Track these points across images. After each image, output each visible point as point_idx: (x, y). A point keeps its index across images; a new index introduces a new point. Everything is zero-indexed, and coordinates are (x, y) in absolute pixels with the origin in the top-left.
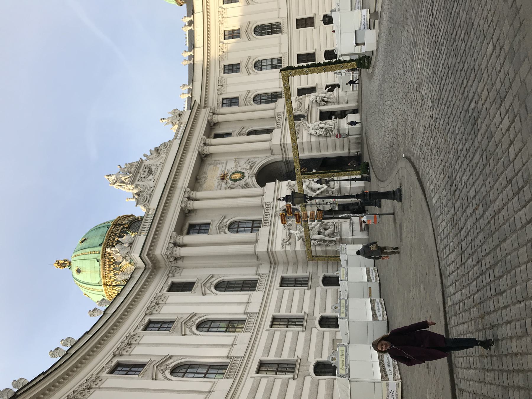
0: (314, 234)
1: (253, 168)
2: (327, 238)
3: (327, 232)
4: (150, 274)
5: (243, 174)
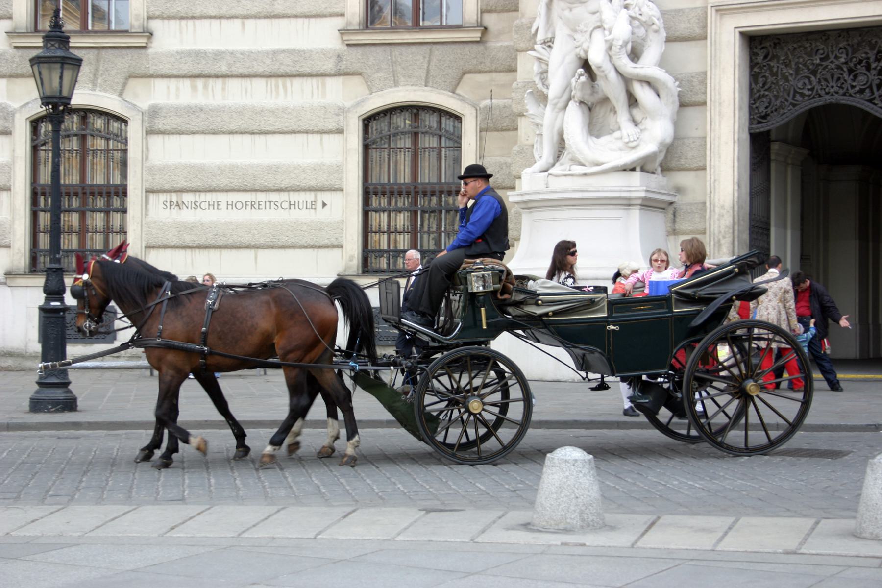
3: (574, 121)
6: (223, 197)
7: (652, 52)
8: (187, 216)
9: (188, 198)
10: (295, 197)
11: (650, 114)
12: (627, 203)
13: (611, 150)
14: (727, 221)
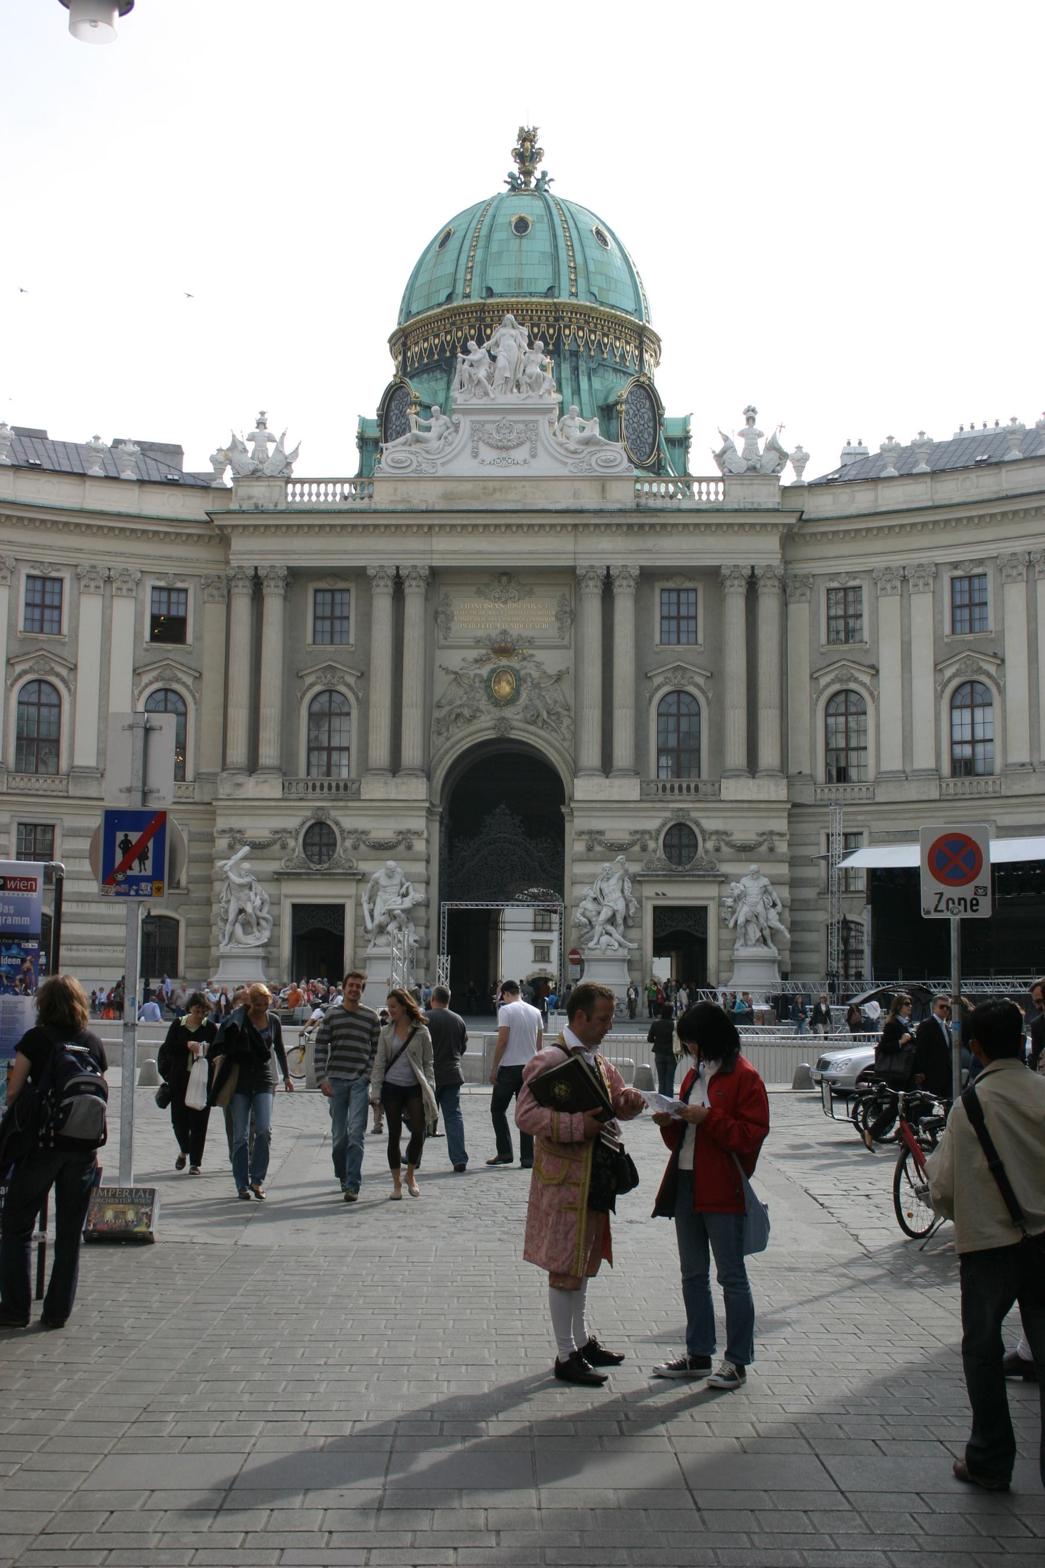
0: (238, 899)
1: (532, 728)
2: (228, 927)
3: (239, 929)
4: (199, 536)
5: (512, 700)
6: (88, 947)
7: (266, 909)
8: (74, 954)
9: (74, 947)
10: (115, 948)
11: (264, 928)
12: (258, 957)
13: (252, 940)
14: (286, 963)
